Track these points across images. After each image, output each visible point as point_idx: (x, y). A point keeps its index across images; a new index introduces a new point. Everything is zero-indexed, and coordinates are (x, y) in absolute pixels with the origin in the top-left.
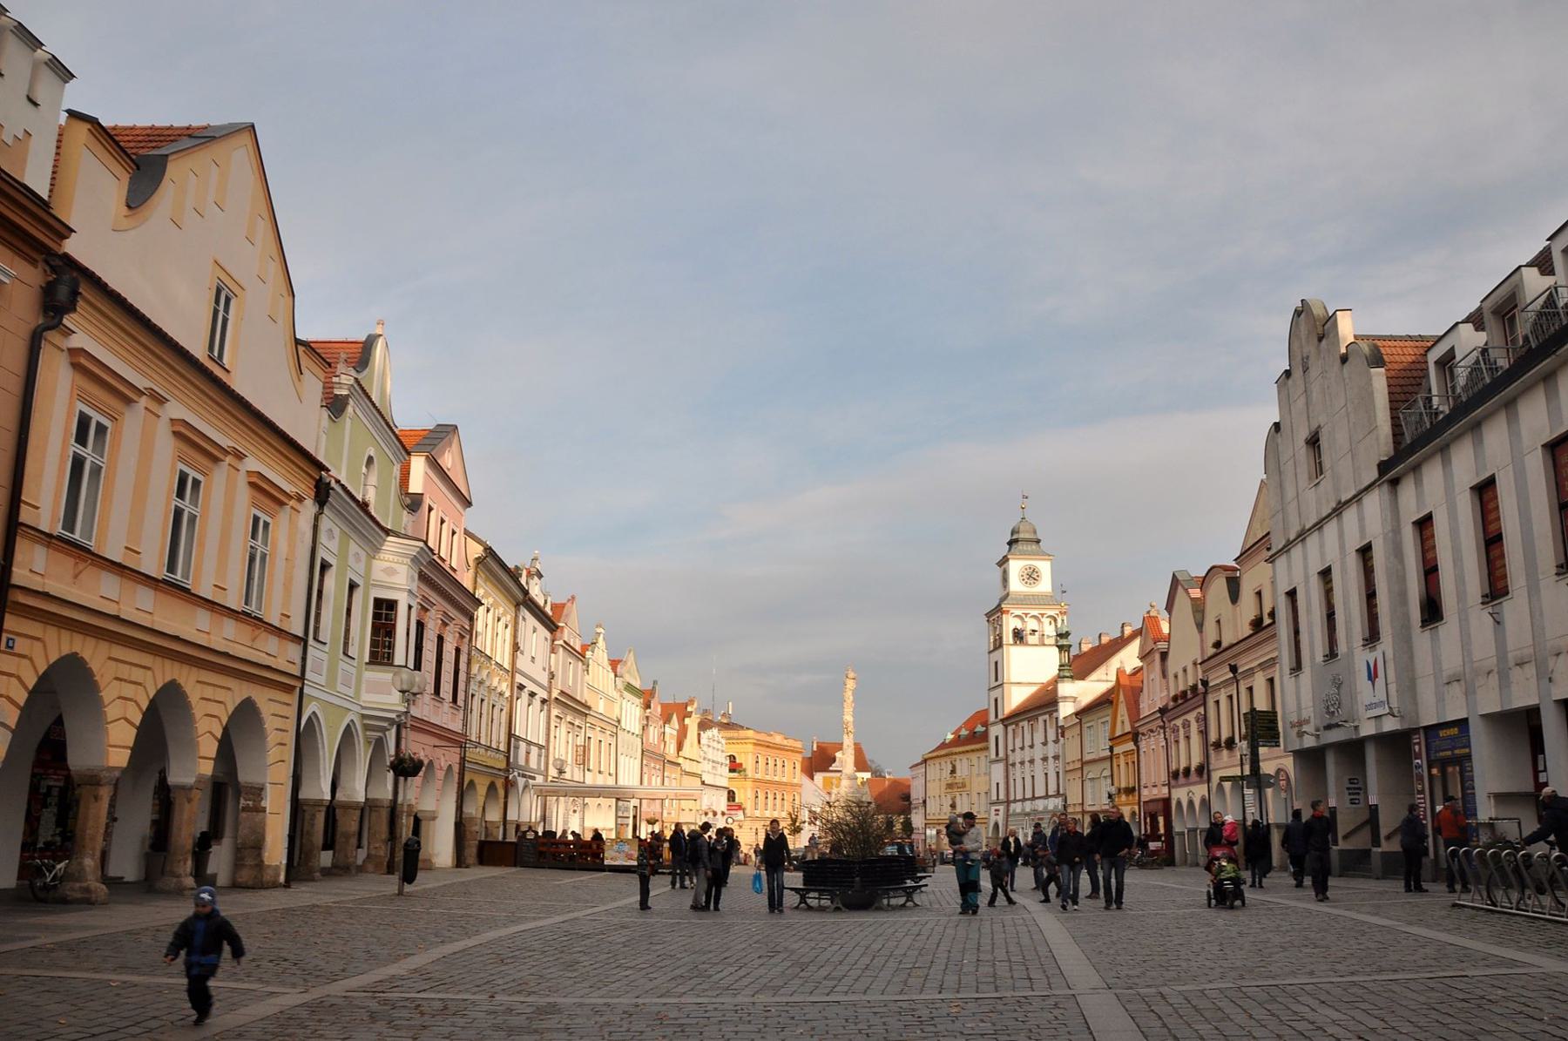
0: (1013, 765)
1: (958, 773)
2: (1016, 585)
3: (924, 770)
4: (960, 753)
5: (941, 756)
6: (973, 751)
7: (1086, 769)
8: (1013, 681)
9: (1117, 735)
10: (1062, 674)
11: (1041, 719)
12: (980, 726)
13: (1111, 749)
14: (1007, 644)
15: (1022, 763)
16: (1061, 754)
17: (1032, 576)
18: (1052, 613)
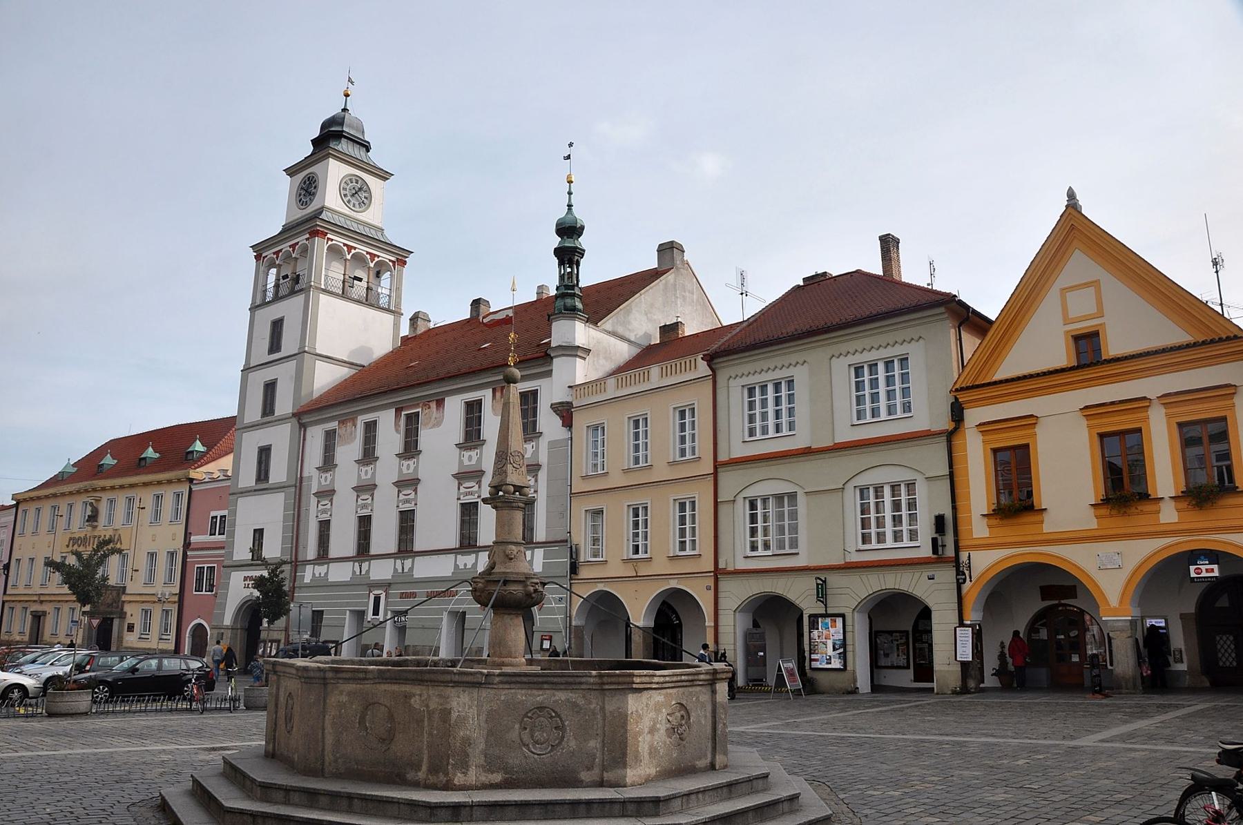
0: (327, 494)
1: (102, 519)
2: (332, 198)
3: (13, 517)
4: (113, 488)
5: (63, 495)
6: (145, 484)
7: (726, 478)
8: (318, 351)
9: (997, 377)
10: (569, 301)
11: (455, 407)
12: (150, 449)
13: (957, 413)
14: (317, 288)
15: (366, 489)
16: (543, 459)
17: (357, 193)
18: (386, 257)
